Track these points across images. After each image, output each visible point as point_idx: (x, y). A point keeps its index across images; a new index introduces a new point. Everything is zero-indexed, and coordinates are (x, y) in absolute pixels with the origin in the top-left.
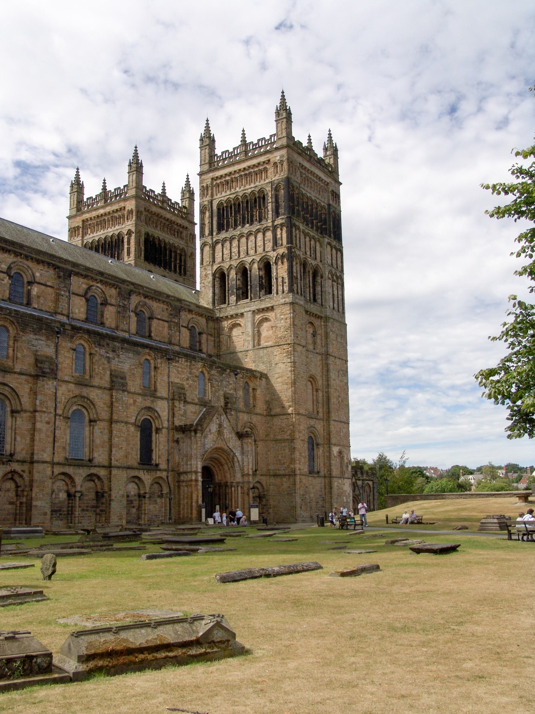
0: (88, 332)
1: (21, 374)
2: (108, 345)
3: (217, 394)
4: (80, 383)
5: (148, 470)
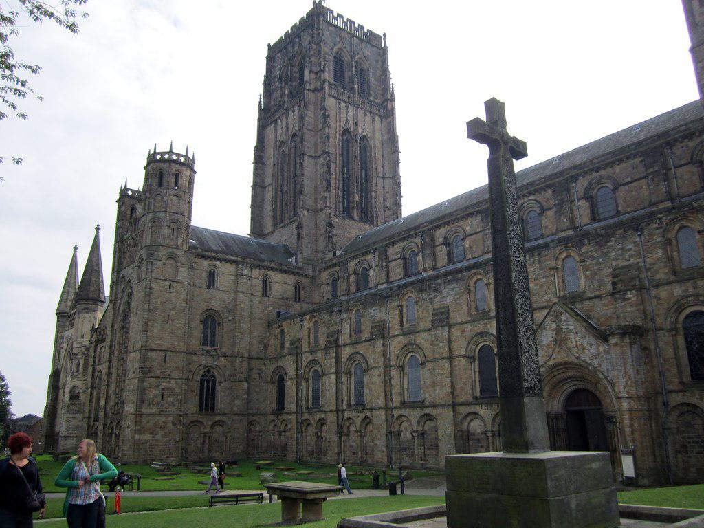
0: (412, 284)
1: (366, 341)
2: (430, 286)
3: (597, 277)
4: (405, 334)
5: (487, 405)
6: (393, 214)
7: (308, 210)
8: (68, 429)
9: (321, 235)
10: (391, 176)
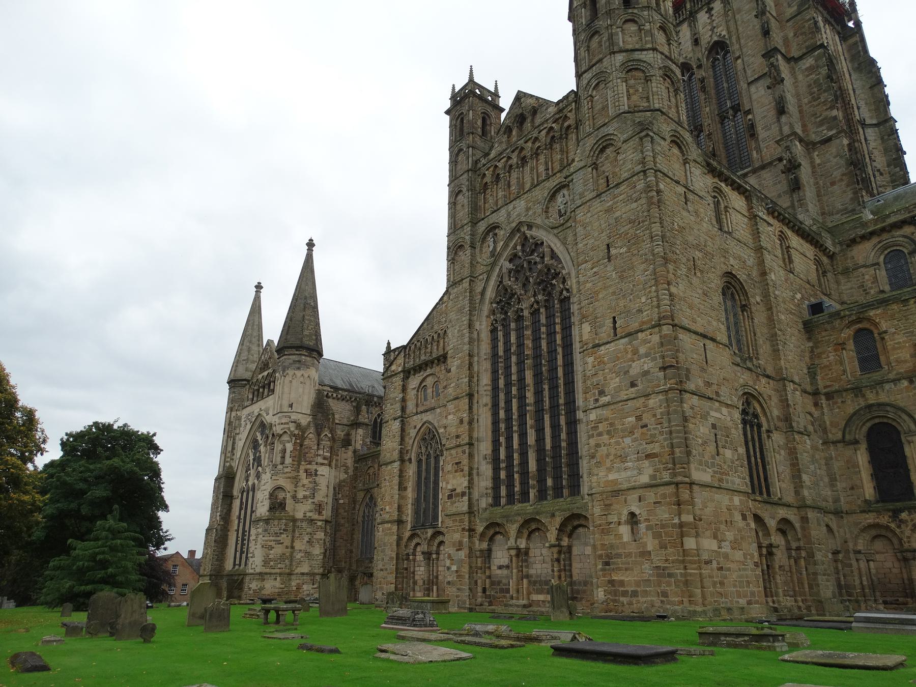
6: (893, 181)
7: (801, 141)
8: (266, 562)
9: (833, 184)
10: (874, 122)
